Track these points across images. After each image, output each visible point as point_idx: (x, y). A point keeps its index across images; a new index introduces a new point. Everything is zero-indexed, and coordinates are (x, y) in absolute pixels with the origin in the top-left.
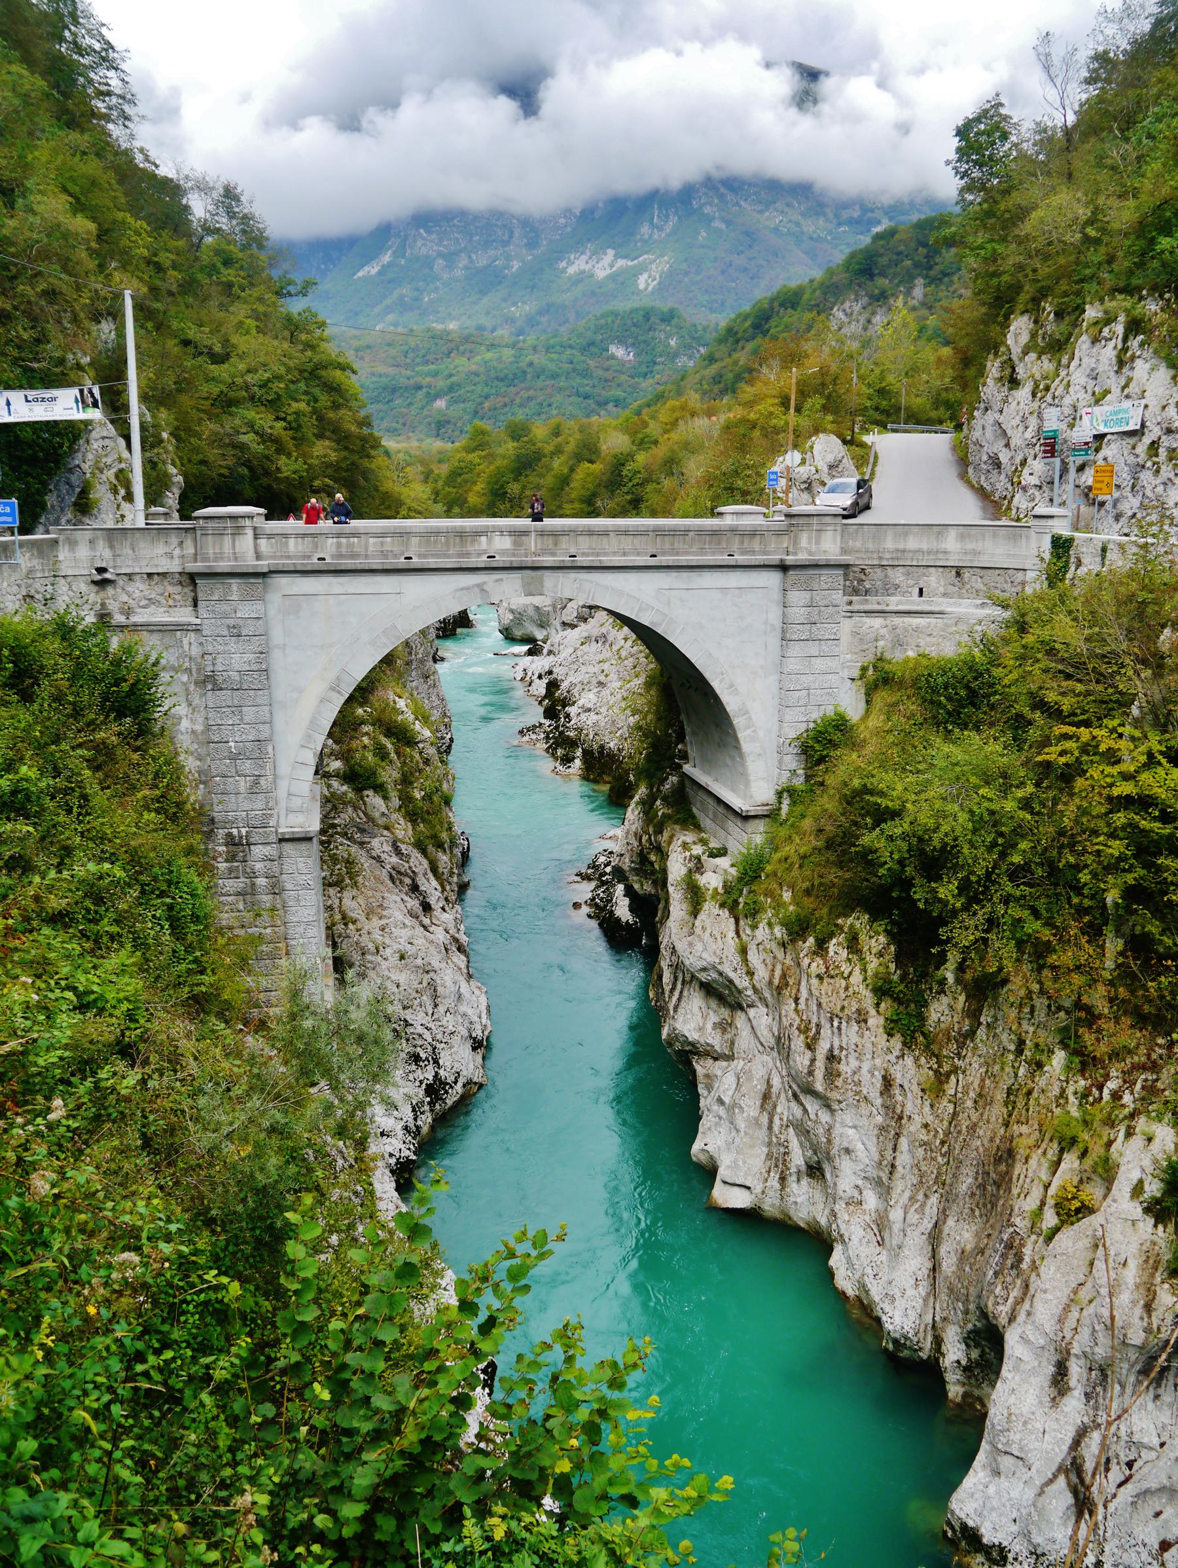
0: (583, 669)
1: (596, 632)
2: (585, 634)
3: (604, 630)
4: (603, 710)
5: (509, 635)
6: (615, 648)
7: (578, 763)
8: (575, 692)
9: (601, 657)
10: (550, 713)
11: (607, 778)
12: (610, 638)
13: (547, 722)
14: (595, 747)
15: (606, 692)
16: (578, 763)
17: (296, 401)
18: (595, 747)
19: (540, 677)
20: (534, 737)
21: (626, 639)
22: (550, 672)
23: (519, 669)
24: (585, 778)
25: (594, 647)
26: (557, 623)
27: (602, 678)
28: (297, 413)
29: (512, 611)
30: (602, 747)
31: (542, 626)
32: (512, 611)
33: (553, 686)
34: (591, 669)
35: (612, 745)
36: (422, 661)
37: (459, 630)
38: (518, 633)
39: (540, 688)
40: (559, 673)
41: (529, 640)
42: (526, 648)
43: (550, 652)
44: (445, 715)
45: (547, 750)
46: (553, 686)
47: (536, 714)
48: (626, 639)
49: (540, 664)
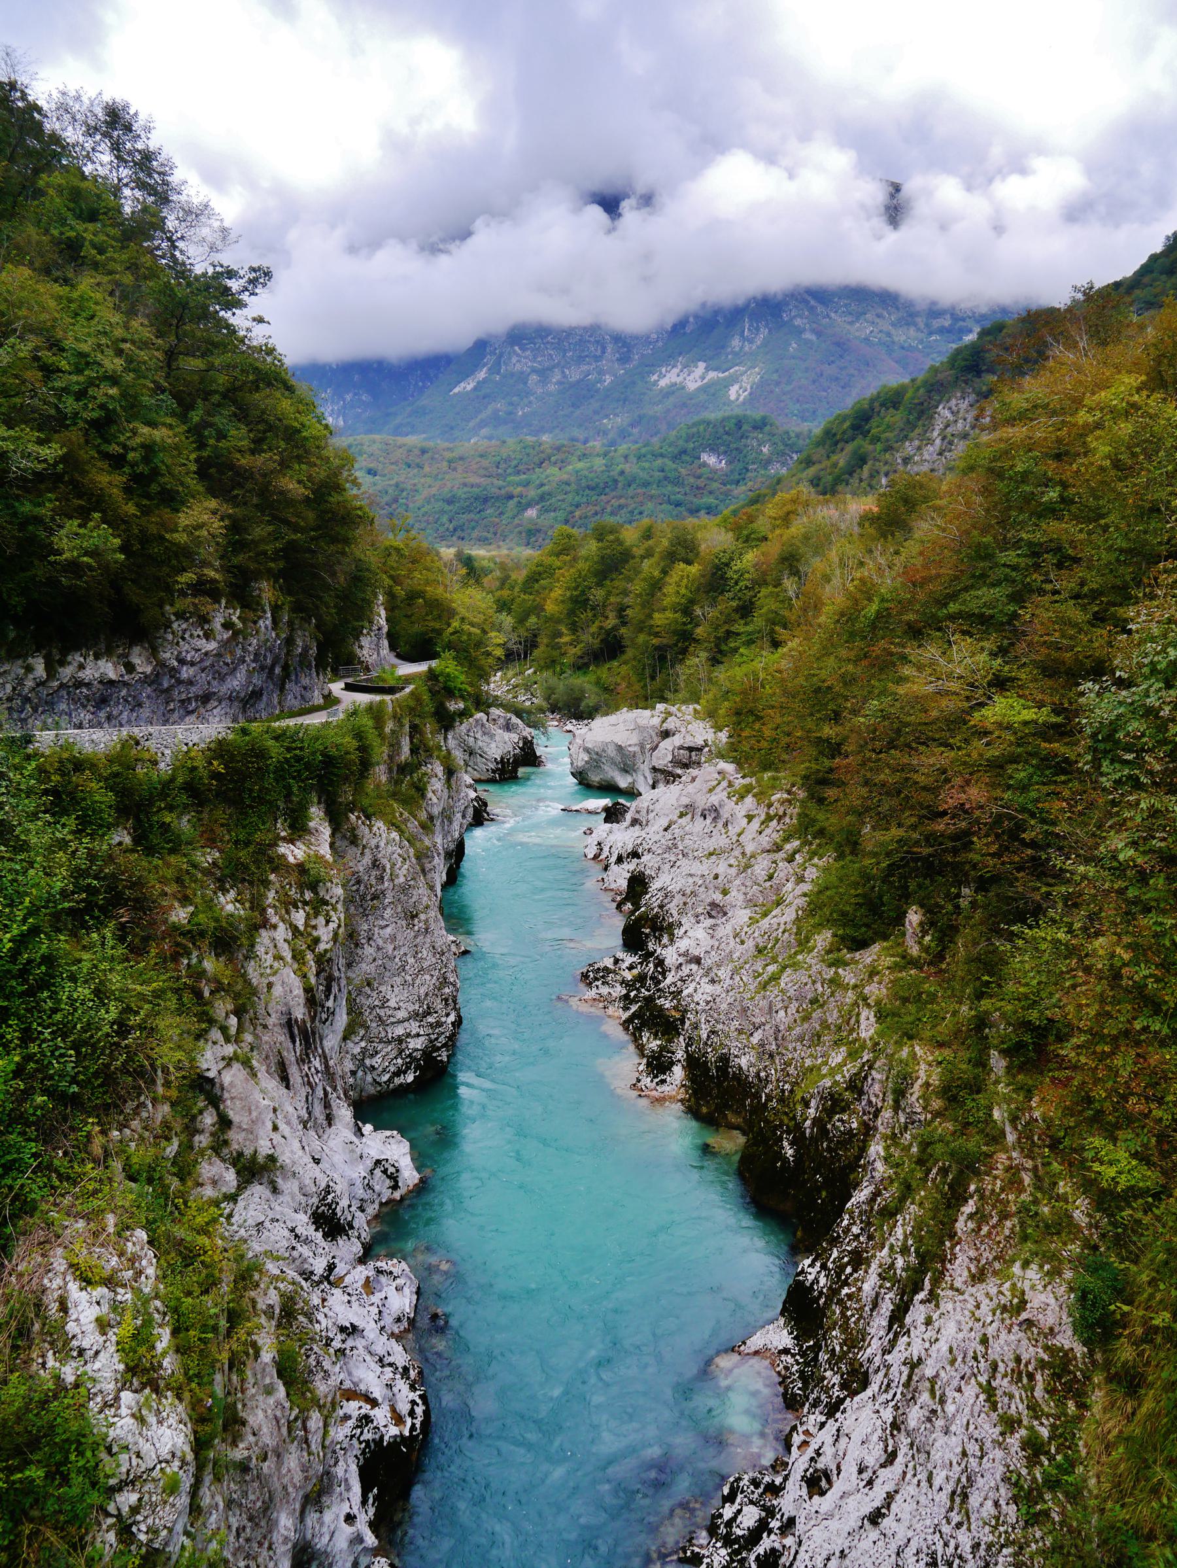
0: (683, 862)
1: (703, 801)
2: (685, 801)
3: (714, 799)
4: (723, 973)
5: (585, 782)
6: (733, 830)
7: (678, 1072)
8: (673, 908)
9: (711, 844)
10: (633, 939)
11: (733, 1119)
12: (725, 814)
13: (629, 959)
14: (711, 1057)
17: (152, 424)
19: (620, 860)
20: (605, 990)
21: (750, 818)
22: (635, 855)
23: (592, 840)
24: (693, 1111)
25: (700, 825)
26: (645, 768)
27: (718, 897)
28: (149, 449)
29: (587, 750)
30: (725, 1059)
31: (626, 770)
32: (587, 750)
35: (744, 1062)
36: (405, 889)
37: (521, 771)
38: (595, 778)
39: (619, 877)
40: (648, 862)
41: (608, 788)
42: (606, 802)
43: (635, 822)
44: (444, 981)
45: (626, 1024)
46: (638, 884)
47: (605, 940)
48: (750, 818)
49: (621, 837)
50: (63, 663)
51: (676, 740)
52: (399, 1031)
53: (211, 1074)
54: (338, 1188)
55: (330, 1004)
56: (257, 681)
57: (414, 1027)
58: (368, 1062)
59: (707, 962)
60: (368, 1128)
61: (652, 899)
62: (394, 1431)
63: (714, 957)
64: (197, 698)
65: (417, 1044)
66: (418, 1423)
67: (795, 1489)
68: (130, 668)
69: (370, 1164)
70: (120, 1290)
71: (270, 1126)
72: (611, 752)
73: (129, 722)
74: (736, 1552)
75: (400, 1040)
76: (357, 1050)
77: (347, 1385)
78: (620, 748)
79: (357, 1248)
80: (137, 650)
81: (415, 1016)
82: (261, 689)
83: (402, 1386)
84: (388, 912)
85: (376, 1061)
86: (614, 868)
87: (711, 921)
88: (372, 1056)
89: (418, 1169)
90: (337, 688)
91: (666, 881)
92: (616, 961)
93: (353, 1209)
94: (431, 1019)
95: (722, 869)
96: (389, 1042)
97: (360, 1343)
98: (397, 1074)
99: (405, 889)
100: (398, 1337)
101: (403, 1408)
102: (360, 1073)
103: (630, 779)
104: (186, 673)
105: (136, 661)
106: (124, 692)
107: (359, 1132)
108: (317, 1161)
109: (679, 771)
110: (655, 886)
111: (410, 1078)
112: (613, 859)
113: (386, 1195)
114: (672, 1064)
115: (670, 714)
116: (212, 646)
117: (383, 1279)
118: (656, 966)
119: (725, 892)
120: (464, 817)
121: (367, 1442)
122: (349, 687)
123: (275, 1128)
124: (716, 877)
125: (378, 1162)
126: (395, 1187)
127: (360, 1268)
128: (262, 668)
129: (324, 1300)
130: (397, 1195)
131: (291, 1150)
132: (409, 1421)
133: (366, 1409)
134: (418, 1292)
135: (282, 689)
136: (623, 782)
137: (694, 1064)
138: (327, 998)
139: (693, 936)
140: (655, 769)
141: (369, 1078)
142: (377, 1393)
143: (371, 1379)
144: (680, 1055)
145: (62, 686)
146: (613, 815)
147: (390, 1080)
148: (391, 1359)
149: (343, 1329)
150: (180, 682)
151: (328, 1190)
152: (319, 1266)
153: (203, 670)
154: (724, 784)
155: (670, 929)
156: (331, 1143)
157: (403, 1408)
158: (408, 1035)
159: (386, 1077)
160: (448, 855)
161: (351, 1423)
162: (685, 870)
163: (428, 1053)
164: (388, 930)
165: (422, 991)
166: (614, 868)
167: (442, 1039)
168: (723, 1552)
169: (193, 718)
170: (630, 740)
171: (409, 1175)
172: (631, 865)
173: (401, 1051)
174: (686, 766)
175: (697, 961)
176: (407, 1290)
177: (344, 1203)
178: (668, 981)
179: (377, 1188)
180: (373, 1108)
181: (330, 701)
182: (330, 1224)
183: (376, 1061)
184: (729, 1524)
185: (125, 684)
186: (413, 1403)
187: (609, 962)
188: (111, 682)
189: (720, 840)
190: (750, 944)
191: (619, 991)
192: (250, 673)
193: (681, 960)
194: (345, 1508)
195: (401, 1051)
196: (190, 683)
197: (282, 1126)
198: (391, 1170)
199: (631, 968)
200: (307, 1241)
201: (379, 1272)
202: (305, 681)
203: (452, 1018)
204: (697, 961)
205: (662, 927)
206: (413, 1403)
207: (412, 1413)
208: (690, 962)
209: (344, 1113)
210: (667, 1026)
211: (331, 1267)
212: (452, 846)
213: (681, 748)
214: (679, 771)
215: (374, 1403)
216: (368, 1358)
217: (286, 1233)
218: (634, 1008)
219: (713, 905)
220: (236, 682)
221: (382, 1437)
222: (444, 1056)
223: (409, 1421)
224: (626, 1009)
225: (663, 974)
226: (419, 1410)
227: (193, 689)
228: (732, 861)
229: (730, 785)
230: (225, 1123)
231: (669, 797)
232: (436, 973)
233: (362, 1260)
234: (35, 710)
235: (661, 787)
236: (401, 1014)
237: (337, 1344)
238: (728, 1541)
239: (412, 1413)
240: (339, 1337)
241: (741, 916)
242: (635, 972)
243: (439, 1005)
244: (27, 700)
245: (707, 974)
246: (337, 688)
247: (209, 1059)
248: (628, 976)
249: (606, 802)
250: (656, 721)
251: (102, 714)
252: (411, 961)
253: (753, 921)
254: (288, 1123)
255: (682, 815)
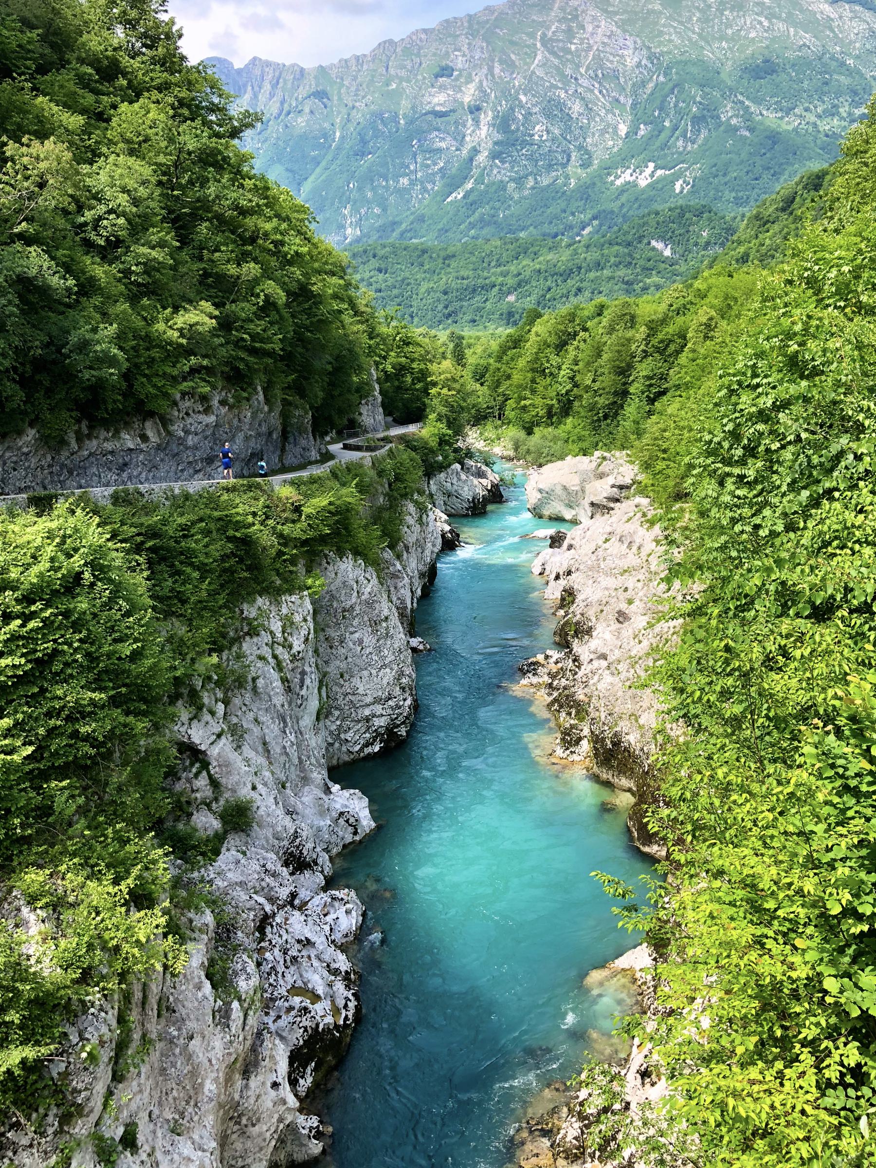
2: (609, 529)
7: (585, 743)
8: (591, 613)
9: (625, 564)
13: (555, 655)
15: (627, 630)
16: (585, 746)
18: (608, 734)
19: (557, 577)
20: (535, 680)
26: (586, 503)
27: (623, 606)
29: (540, 491)
32: (540, 491)
33: (569, 596)
34: (611, 582)
37: (490, 507)
38: (546, 512)
40: (576, 580)
43: (570, 547)
46: (569, 596)
50: (89, 437)
51: (610, 480)
52: (367, 712)
53: (203, 748)
54: (304, 834)
55: (303, 692)
56: (255, 445)
57: (378, 709)
58: (342, 736)
59: (611, 658)
60: (335, 788)
61: (577, 608)
62: (329, 1019)
63: (617, 653)
64: (202, 460)
65: (380, 722)
66: (350, 1015)
67: (632, 1078)
68: (144, 438)
69: (335, 815)
70: (123, 909)
71: (249, 786)
72: (559, 491)
73: (147, 479)
74: (587, 1126)
75: (367, 720)
76: (333, 727)
77: (299, 983)
78: (565, 488)
79: (320, 879)
80: (148, 424)
81: (377, 701)
82: (262, 451)
83: (340, 986)
84: (355, 622)
85: (349, 736)
86: (552, 583)
87: (618, 625)
88: (346, 732)
89: (374, 818)
90: (335, 448)
91: (589, 593)
92: (547, 657)
93: (318, 849)
94: (390, 703)
95: (631, 583)
96: (359, 721)
97: (313, 953)
98: (367, 744)
99: (370, 604)
100: (343, 948)
101: (341, 1003)
102: (337, 745)
103: (574, 512)
104: (191, 441)
105: (150, 433)
106: (141, 457)
107: (327, 791)
108: (289, 813)
109: (612, 505)
110: (580, 598)
111: (377, 749)
112: (553, 576)
113: (349, 838)
114: (580, 739)
115: (604, 458)
116: (212, 419)
117: (336, 904)
118: (574, 661)
119: (630, 602)
120: (434, 545)
121: (306, 1028)
122: (346, 447)
123: (254, 788)
124: (626, 590)
125: (341, 814)
126: (355, 833)
127: (322, 895)
128: (259, 435)
129: (287, 919)
130: (357, 838)
131: (266, 805)
132: (344, 1012)
133: (307, 1003)
134: (364, 915)
135: (283, 450)
136: (568, 515)
137: (597, 740)
138: (301, 687)
139: (604, 636)
140: (592, 504)
141: (344, 749)
142: (320, 991)
143: (317, 980)
144: (586, 732)
145: (91, 454)
146: (556, 541)
147: (361, 750)
148: (336, 966)
149: (299, 941)
150: (187, 448)
151: (296, 835)
152: (283, 893)
153: (206, 438)
154: (639, 515)
155: (589, 631)
156: (305, 799)
157: (341, 1003)
158: (374, 716)
159: (357, 748)
160: (422, 575)
161: (293, 1013)
162: (604, 584)
163: (390, 731)
164: (357, 635)
165: (385, 681)
166: (552, 583)
167: (401, 719)
168: (577, 1125)
169: (201, 475)
170: (573, 483)
171: (367, 823)
172: (562, 583)
173: (368, 728)
174: (617, 500)
175: (604, 657)
176: (354, 913)
177: (310, 845)
178: (580, 673)
179: (341, 833)
180: (343, 773)
181: (327, 457)
182: (297, 863)
183: (349, 736)
184: (582, 1104)
185: (142, 451)
186: (347, 999)
187: (540, 658)
188: (131, 450)
189: (632, 560)
190: (645, 643)
191: (547, 679)
192: (247, 438)
193: (592, 656)
194: (273, 1078)
195: (368, 728)
196: (195, 448)
197: (260, 787)
198: (352, 820)
199: (556, 663)
200: (274, 875)
201: (334, 899)
202: (303, 442)
203: (409, 702)
204: (604, 657)
205: (582, 631)
206: (347, 999)
207: (346, 1006)
208: (599, 658)
209: (319, 775)
210: (580, 710)
211: (293, 895)
212: (424, 569)
213: (613, 486)
214: (612, 505)
215: (316, 998)
216: (316, 963)
217: (258, 868)
218: (555, 694)
219: (621, 613)
220: (235, 446)
221: (317, 1025)
222: (403, 731)
223: (344, 1012)
224: (550, 694)
225: (579, 667)
226: (352, 1005)
227: (198, 453)
228: (641, 577)
229: (644, 515)
230: (214, 783)
231: (601, 524)
232: (395, 667)
233: (325, 889)
234: (71, 472)
235: (598, 516)
236: (369, 699)
237: (293, 952)
238: (581, 1117)
239: (346, 1006)
240: (298, 946)
241: (639, 622)
242: (560, 665)
243: (397, 691)
244: (63, 466)
245: (608, 668)
246: (335, 448)
247: (198, 735)
248: (554, 668)
249: (551, 531)
250: (594, 464)
251: (125, 475)
252: (375, 658)
253: (651, 625)
254: (265, 784)
255: (607, 540)
